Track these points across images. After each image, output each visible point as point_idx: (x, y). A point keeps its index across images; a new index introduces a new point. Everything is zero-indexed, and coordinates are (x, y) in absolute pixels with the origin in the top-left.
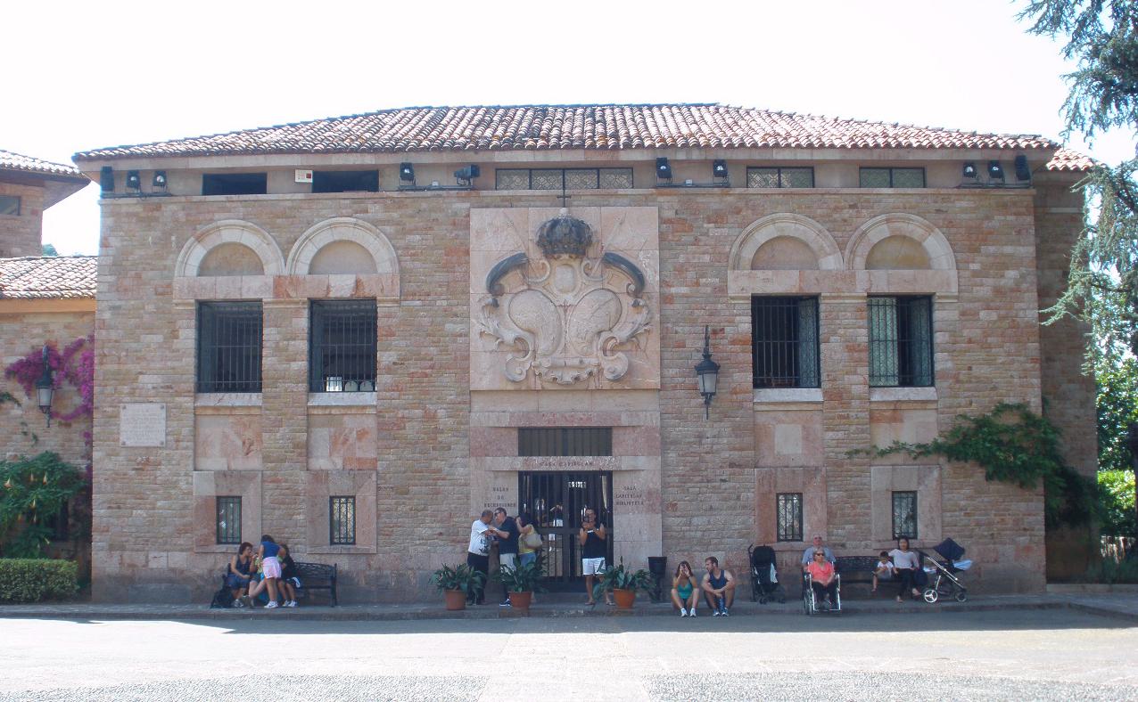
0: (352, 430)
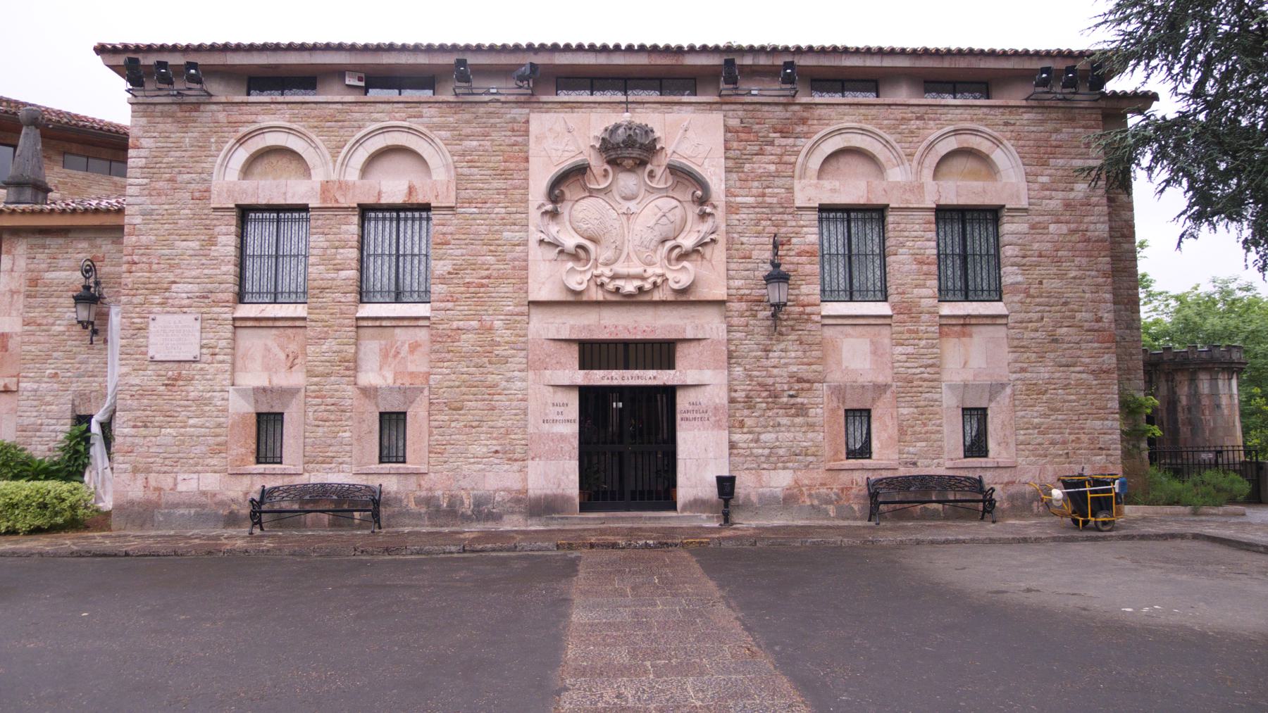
0: (403, 343)
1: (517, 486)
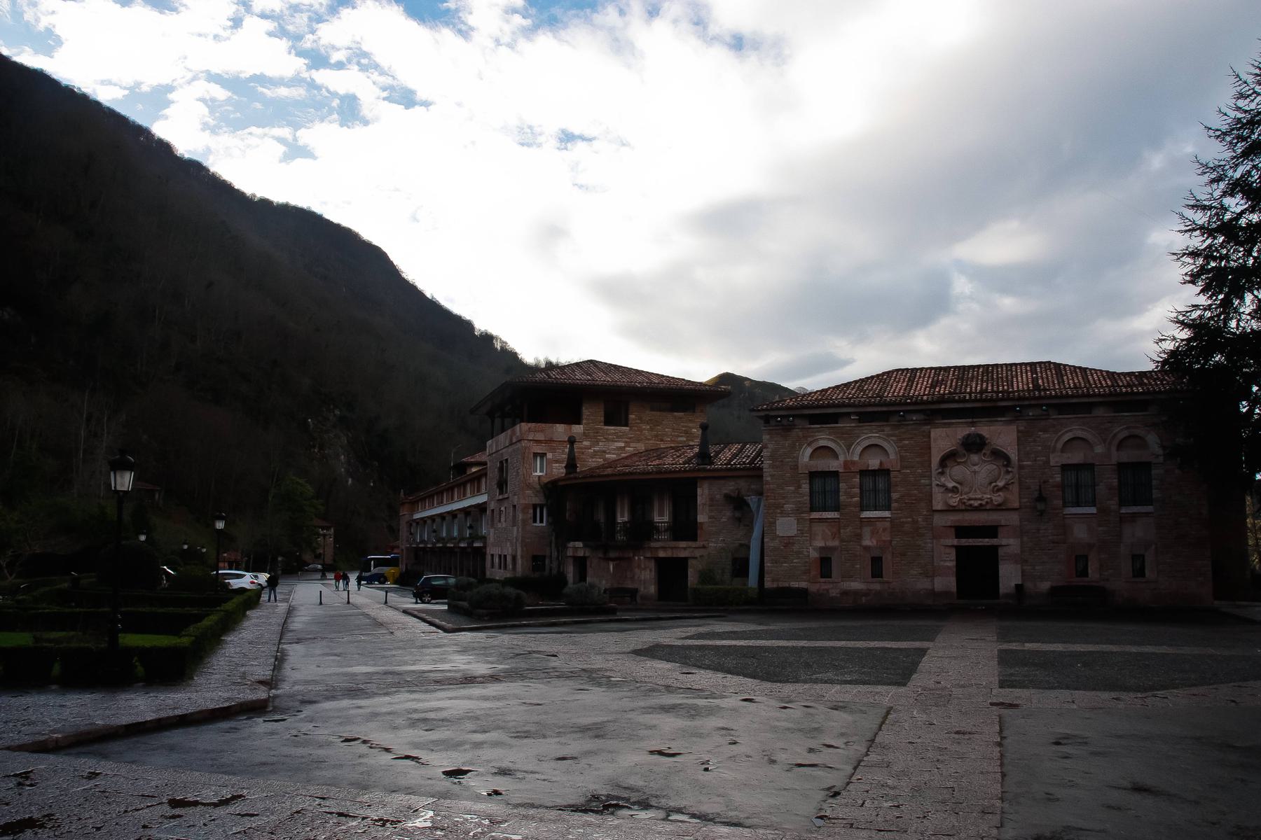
1: (930, 587)
